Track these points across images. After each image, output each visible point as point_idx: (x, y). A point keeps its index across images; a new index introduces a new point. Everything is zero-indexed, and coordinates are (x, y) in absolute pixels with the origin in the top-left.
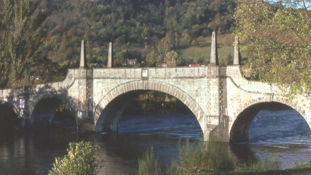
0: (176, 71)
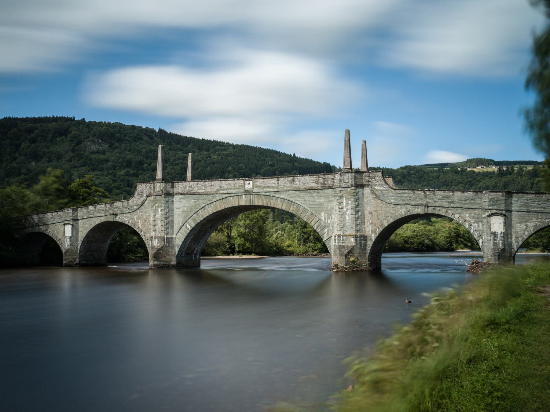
0: (293, 180)
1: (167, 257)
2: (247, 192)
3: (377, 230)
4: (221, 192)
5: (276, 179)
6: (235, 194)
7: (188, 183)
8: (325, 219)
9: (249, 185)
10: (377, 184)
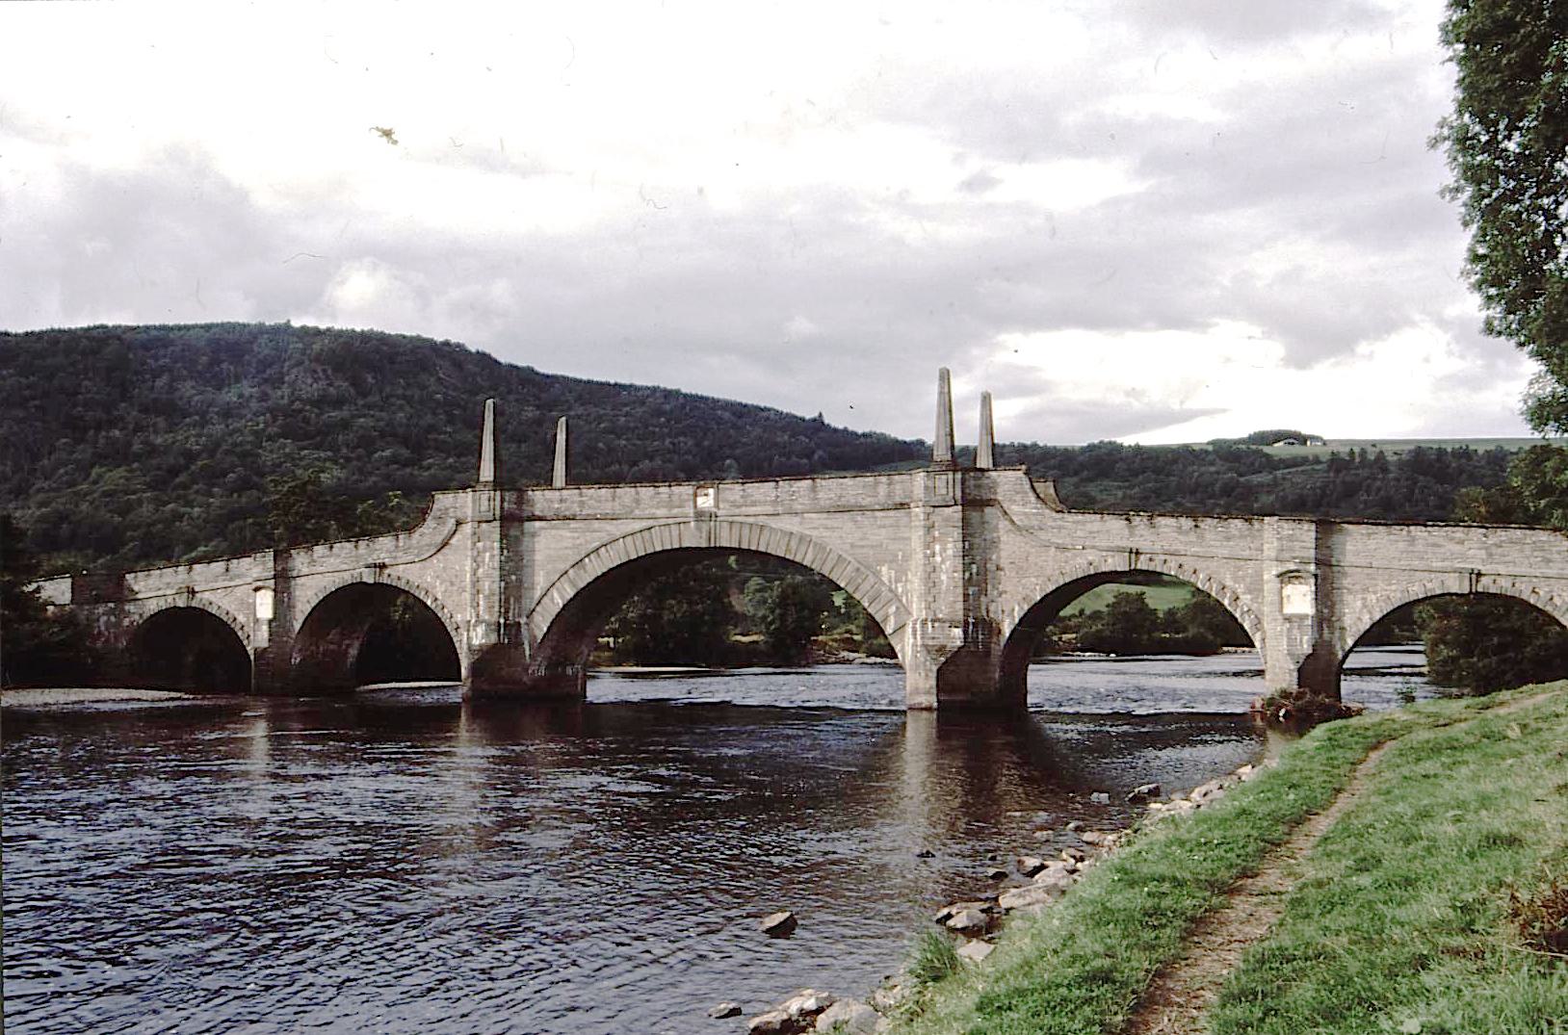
0: (814, 489)
3: (1017, 608)
5: (773, 484)
7: (557, 493)
8: (890, 582)
9: (706, 501)
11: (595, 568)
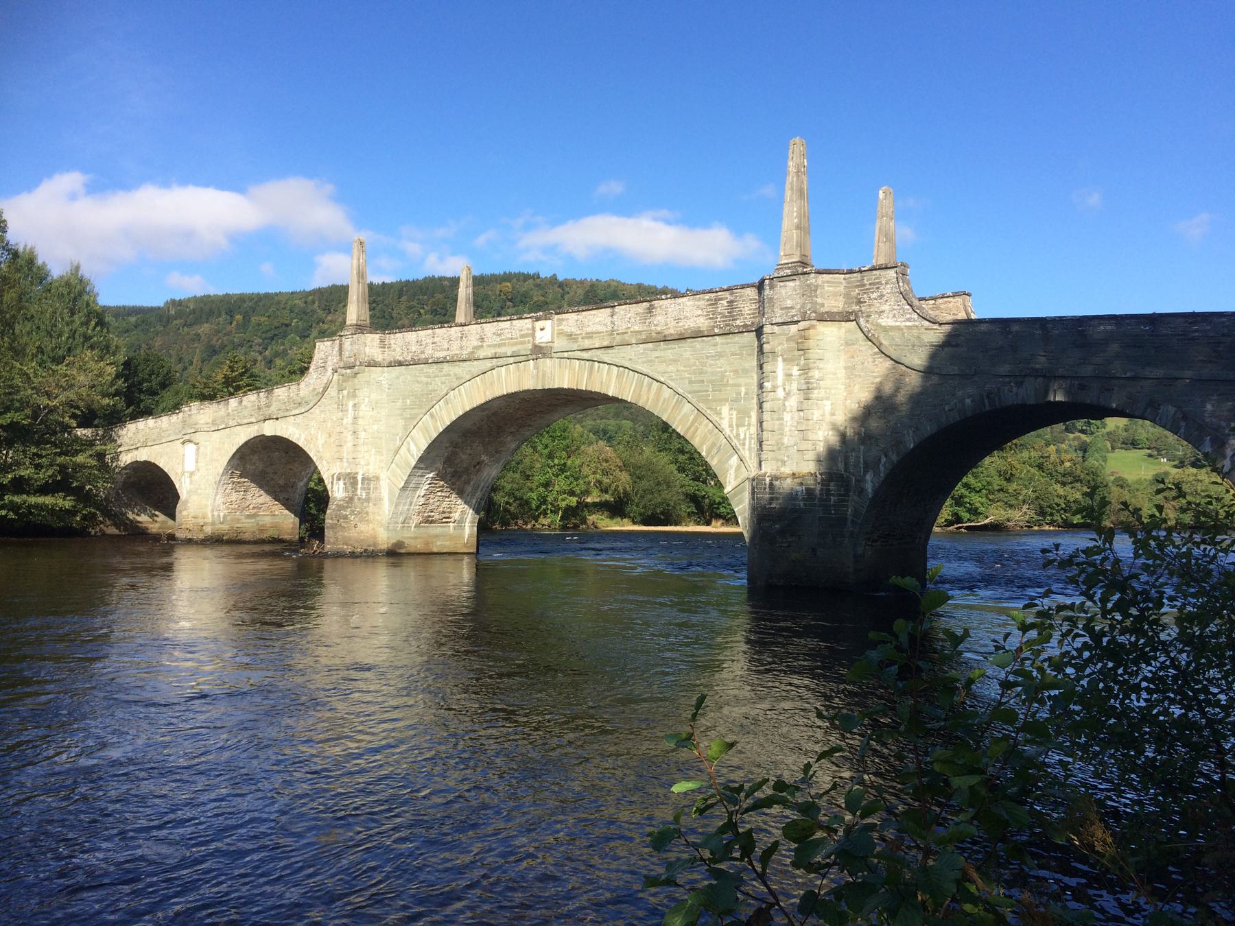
0: (650, 310)
1: (362, 527)
2: (539, 352)
3: (884, 459)
4: (481, 354)
5: (608, 310)
6: (511, 360)
8: (731, 426)
10: (886, 307)
11: (447, 414)
